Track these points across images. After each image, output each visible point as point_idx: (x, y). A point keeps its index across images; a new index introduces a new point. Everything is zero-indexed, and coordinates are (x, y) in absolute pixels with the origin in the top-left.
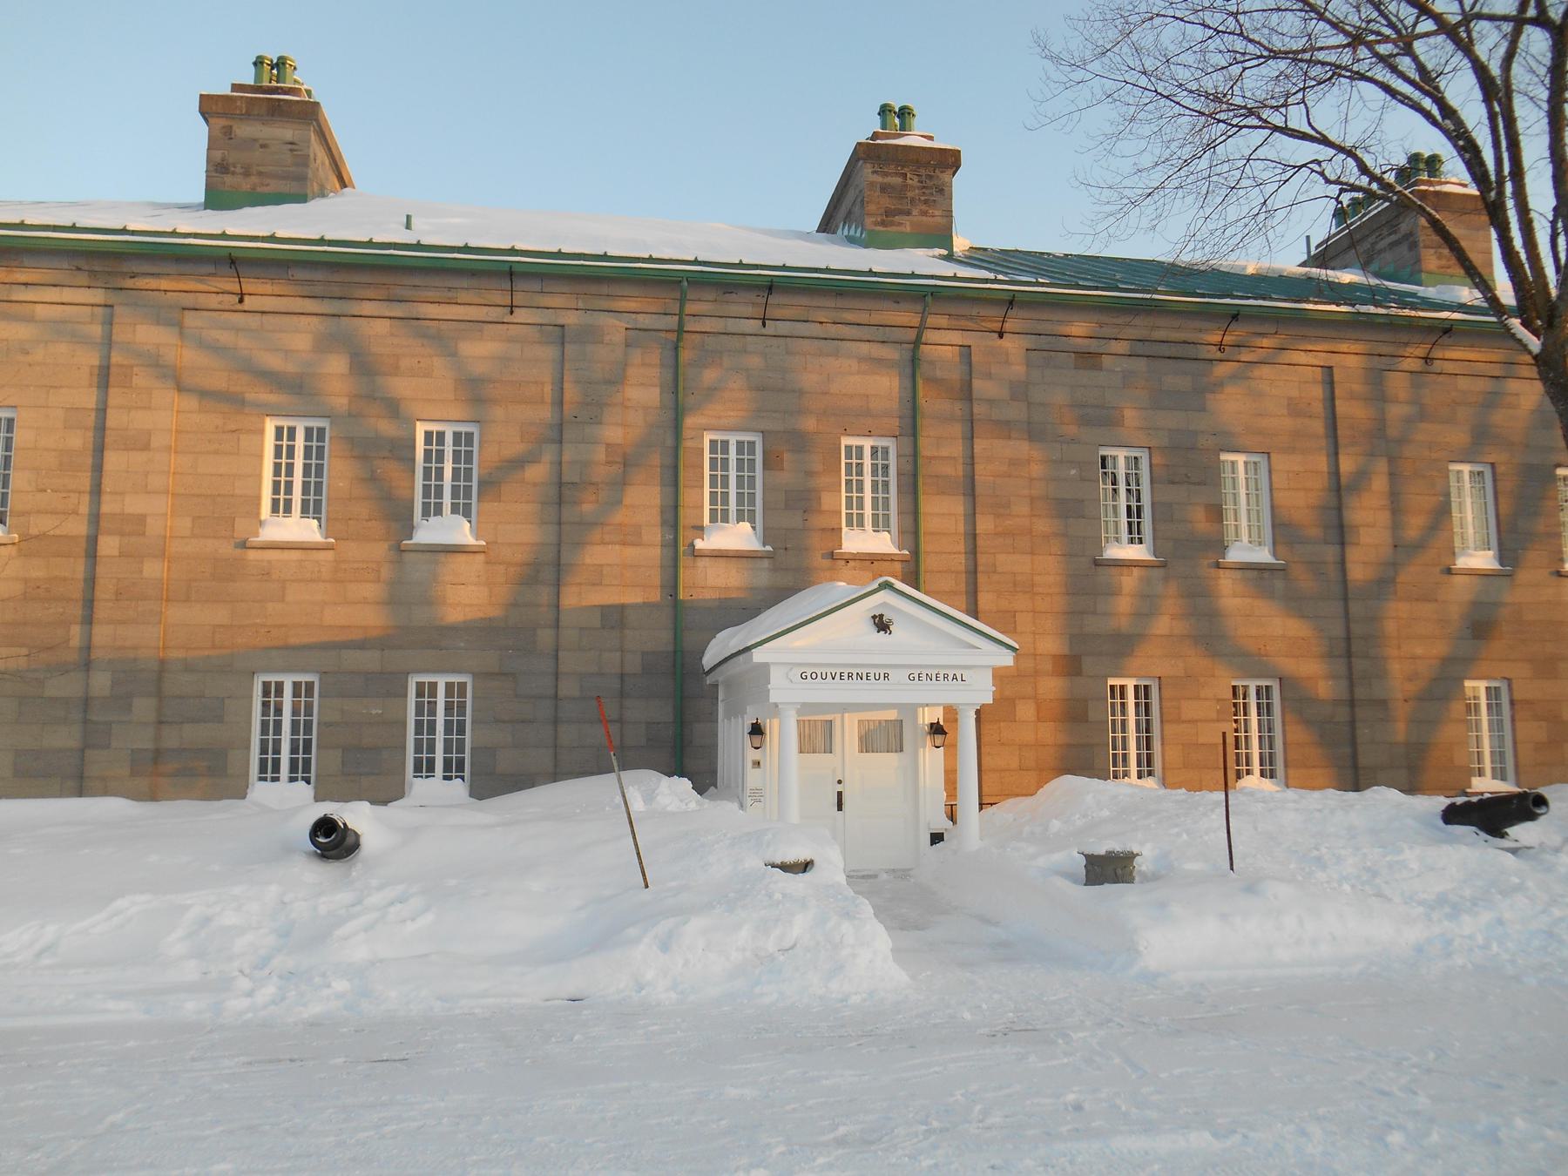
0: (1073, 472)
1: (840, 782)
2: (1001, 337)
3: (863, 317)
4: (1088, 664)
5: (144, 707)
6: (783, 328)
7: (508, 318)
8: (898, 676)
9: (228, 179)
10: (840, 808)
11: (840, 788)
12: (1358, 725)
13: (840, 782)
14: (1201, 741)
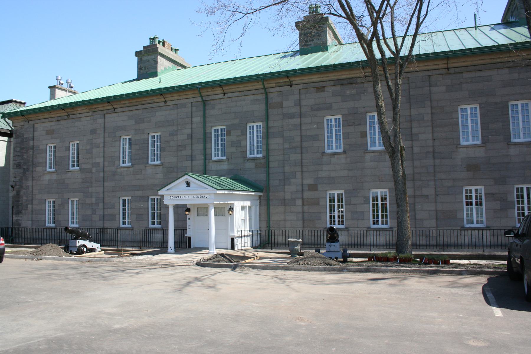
2: (291, 87)
3: (251, 88)
4: (320, 187)
5: (101, 205)
6: (230, 95)
7: (165, 105)
8: (191, 197)
9: (141, 71)
12: (416, 204)
14: (358, 210)
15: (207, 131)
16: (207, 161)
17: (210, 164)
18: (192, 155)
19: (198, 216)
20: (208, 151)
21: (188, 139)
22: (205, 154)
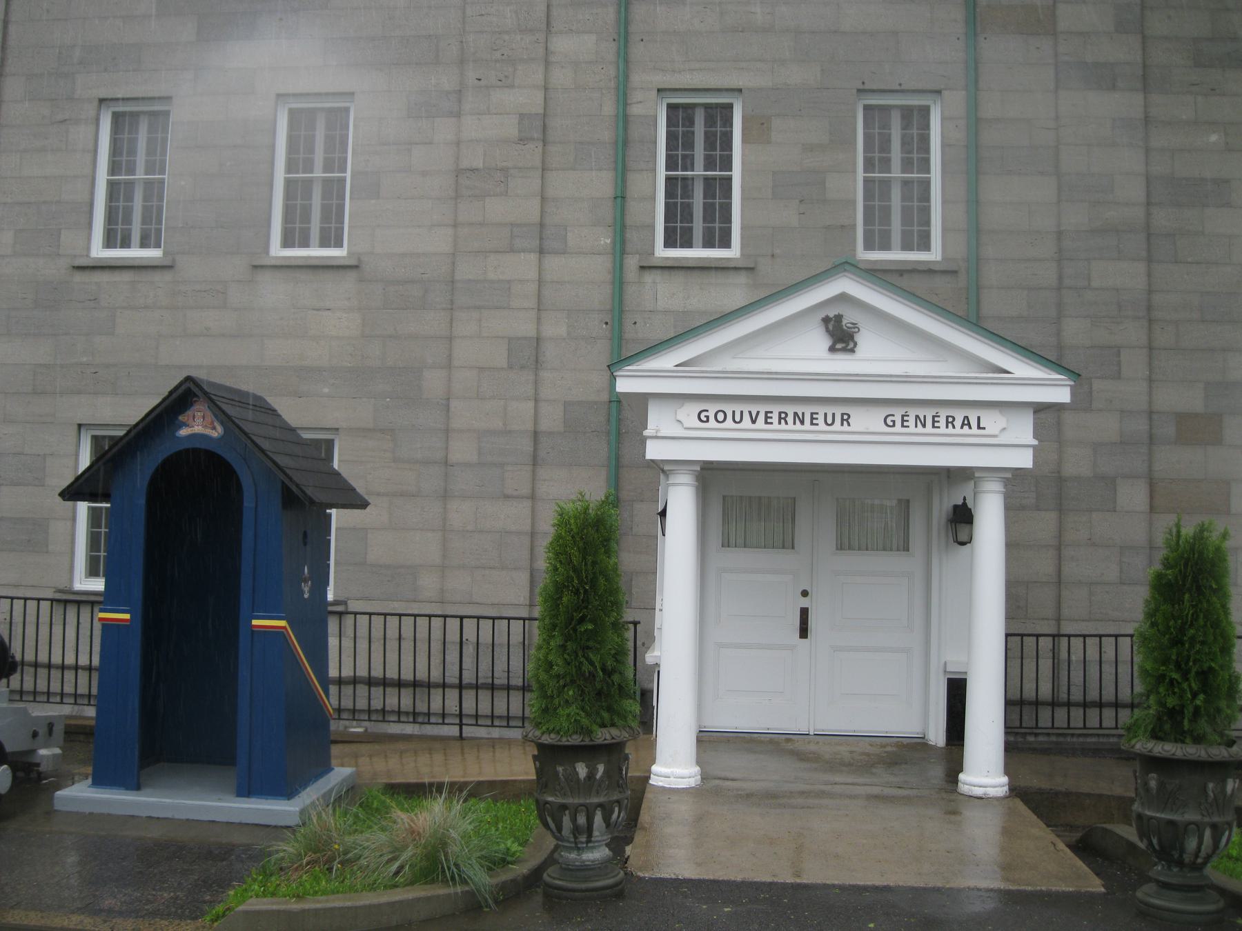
0: (1214, 138)
1: (805, 594)
10: (804, 632)
11: (804, 602)
13: (805, 594)
15: (635, 110)
16: (632, 262)
17: (649, 277)
18: (542, 225)
19: (840, 547)
20: (635, 211)
21: (522, 140)
22: (621, 229)
